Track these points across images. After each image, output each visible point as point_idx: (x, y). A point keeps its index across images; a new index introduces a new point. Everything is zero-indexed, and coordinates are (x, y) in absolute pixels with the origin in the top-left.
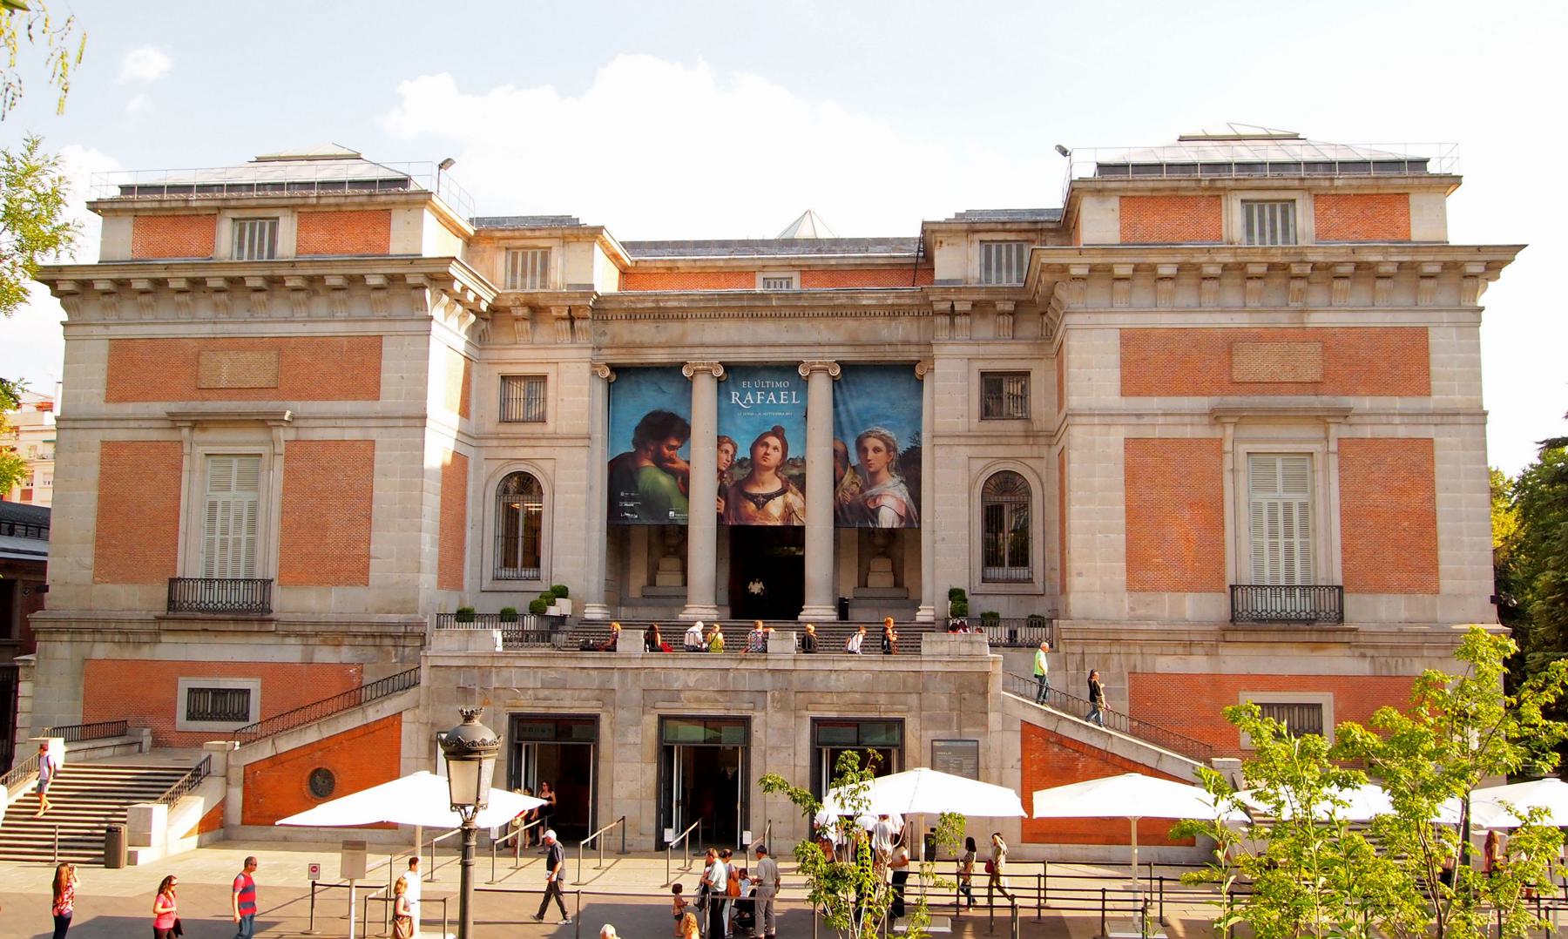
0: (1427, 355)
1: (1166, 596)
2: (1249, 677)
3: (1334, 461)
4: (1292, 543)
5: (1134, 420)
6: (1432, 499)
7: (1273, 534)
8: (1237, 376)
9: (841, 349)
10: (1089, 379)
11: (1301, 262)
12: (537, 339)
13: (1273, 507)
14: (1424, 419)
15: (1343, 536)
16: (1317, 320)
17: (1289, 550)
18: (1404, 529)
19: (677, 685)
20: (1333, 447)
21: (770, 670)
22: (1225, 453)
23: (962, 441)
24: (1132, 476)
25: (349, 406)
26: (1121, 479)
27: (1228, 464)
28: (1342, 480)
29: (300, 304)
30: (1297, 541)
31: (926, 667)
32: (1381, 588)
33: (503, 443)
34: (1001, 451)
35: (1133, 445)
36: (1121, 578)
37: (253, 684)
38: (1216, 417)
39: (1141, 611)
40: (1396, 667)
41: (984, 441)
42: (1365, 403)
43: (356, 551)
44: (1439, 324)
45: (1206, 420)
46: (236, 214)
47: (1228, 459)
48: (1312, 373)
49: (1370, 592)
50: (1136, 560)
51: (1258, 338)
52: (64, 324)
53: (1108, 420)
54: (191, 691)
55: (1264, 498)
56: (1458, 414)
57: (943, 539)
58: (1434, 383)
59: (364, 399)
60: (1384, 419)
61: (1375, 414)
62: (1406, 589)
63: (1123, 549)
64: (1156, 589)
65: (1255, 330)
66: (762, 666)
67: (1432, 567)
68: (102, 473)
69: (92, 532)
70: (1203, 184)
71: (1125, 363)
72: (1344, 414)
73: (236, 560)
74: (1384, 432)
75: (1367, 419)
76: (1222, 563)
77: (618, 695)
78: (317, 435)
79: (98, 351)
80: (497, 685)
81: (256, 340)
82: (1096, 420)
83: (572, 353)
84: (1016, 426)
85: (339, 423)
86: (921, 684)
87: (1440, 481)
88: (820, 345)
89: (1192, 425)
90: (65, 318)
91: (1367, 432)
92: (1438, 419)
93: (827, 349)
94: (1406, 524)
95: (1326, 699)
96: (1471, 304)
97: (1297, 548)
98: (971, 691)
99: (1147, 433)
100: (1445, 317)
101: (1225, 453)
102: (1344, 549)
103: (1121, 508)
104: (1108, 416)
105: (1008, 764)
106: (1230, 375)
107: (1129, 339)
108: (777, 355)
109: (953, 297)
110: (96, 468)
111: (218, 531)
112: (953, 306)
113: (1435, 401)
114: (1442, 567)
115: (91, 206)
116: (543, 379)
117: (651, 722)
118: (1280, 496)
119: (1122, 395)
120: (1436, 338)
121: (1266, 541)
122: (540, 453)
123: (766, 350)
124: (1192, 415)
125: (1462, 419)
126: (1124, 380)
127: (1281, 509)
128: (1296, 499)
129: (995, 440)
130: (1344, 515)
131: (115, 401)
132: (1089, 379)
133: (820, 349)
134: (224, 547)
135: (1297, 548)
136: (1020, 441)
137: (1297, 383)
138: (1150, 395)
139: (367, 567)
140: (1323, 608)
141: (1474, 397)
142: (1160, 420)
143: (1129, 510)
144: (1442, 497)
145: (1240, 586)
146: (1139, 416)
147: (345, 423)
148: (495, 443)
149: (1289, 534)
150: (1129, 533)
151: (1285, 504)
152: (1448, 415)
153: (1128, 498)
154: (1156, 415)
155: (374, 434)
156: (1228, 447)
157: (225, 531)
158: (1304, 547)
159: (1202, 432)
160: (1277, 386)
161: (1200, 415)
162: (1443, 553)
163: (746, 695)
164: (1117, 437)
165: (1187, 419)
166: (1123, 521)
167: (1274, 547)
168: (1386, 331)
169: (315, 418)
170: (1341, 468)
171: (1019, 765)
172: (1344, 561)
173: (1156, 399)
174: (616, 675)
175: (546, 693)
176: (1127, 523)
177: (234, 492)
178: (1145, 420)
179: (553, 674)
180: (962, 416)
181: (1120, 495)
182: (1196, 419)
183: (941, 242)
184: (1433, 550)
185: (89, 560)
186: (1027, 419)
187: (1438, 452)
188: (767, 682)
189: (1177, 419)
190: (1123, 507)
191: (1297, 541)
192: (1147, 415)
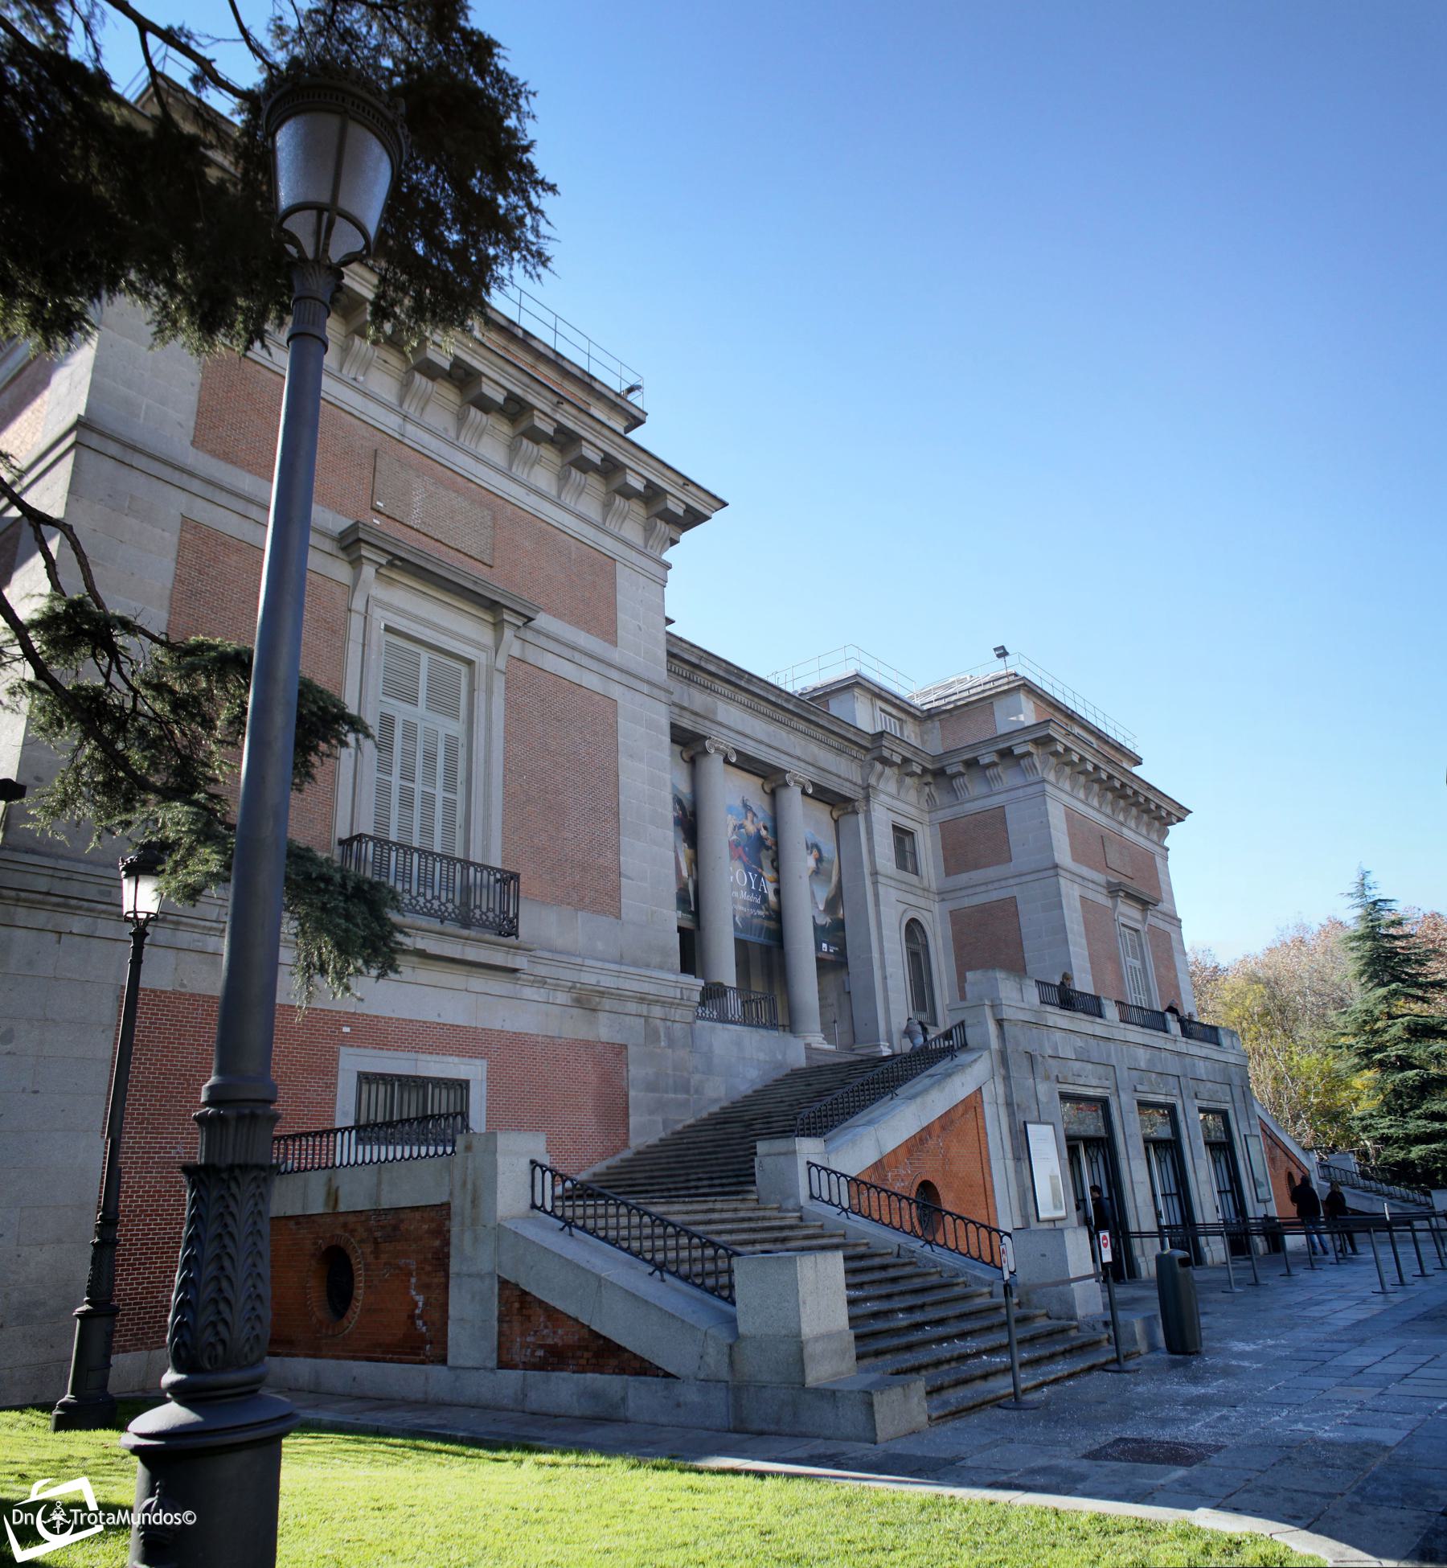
9: (811, 769)
23: (893, 883)
25: (583, 639)
29: (525, 463)
34: (911, 899)
37: (472, 1070)
41: (904, 887)
43: (601, 861)
45: (1105, 891)
54: (365, 1078)
59: (597, 636)
68: (178, 579)
78: (550, 663)
80: (1050, 1052)
81: (459, 479)
84: (912, 878)
85: (577, 657)
111: (396, 770)
129: (908, 888)
131: (213, 453)
134: (407, 801)
136: (920, 892)
139: (618, 888)
147: (585, 661)
155: (616, 692)
157: (408, 775)
169: (548, 636)
186: (916, 872)
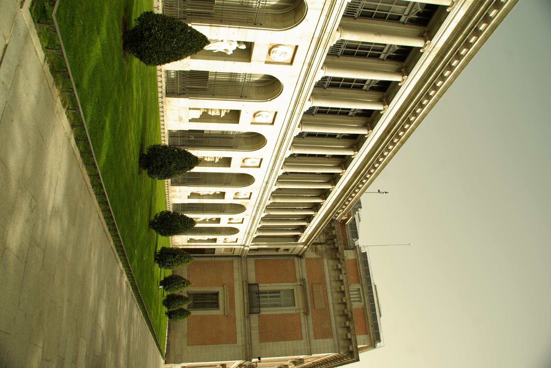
3: (294, 312)
20: (298, 312)
38: (303, 280)
42: (310, 321)
72: (306, 314)
75: (306, 321)
91: (302, 321)
96: (341, 350)
100: (336, 343)
106: (314, 284)
113: (313, 340)
140: (254, 310)
145: (258, 288)
159: (298, 277)
182: (301, 275)
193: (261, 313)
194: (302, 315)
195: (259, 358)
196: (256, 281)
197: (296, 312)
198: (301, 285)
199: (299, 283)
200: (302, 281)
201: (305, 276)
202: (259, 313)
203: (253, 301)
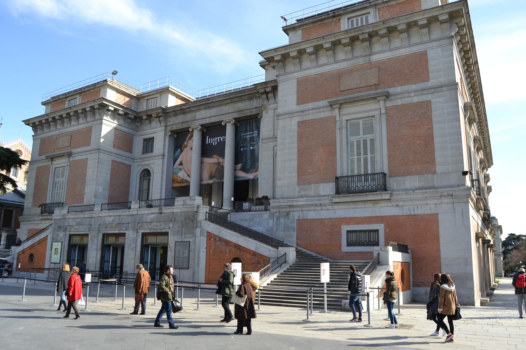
0: (427, 63)
1: (312, 185)
2: (345, 218)
3: (384, 117)
4: (367, 157)
5: (301, 114)
6: (431, 128)
7: (359, 154)
8: (342, 88)
9: (235, 113)
10: (285, 100)
11: (363, 33)
12: (152, 126)
13: (358, 142)
14: (426, 92)
15: (389, 150)
16: (375, 58)
17: (366, 160)
18: (418, 144)
19: (107, 222)
20: (383, 111)
21: (131, 215)
22: (337, 121)
23: (271, 140)
24: (301, 137)
26: (296, 138)
27: (338, 126)
28: (388, 126)
30: (369, 156)
31: (175, 211)
32: (408, 173)
33: (142, 160)
35: (301, 124)
36: (295, 180)
39: (303, 193)
40: (414, 210)
42: (399, 89)
44: (432, 48)
45: (329, 108)
46: (68, 99)
47: (338, 123)
48: (374, 81)
49: (402, 176)
50: (301, 171)
51: (350, 71)
52: (33, 136)
53: (291, 115)
55: (354, 139)
56: (442, 87)
57: (264, 178)
58: (431, 75)
60: (406, 95)
61: (402, 94)
62: (420, 173)
63: (296, 168)
64: (309, 183)
65: (350, 68)
66: (127, 213)
67: (432, 161)
69: (33, 193)
70: (330, 15)
71: (298, 91)
72: (387, 96)
73: (59, 198)
74: (407, 101)
75: (398, 96)
76: (336, 169)
77: (93, 226)
79: (39, 141)
82: (287, 116)
83: (160, 129)
86: (172, 218)
87: (434, 119)
88: (228, 113)
89: (323, 112)
90: (33, 134)
91: (399, 102)
92: (433, 91)
93: (231, 114)
94: (419, 142)
95: (381, 227)
97: (369, 159)
98: (189, 220)
99: (306, 118)
100: (434, 44)
101: (337, 121)
102: (389, 157)
103: (296, 150)
104: (291, 114)
105: (201, 250)
107: (300, 82)
108: (216, 119)
109: (265, 86)
110: (35, 175)
112: (265, 90)
113: (432, 83)
114: (437, 160)
115: (42, 103)
116: (153, 139)
117: (101, 236)
118: (361, 137)
119: (297, 105)
120: (431, 54)
121: (356, 158)
122: (151, 162)
123: (213, 118)
124: (323, 107)
125: (445, 89)
126: (298, 98)
127: (362, 142)
128: (368, 137)
130: (389, 141)
132: (285, 100)
133: (228, 115)
135: (369, 159)
137: (367, 86)
138: (308, 103)
141: (451, 78)
142: (311, 112)
143: (299, 151)
144: (435, 126)
146: (303, 111)
148: (140, 160)
149: (365, 153)
150: (299, 161)
151: (363, 140)
152: (437, 88)
153: (299, 146)
154: (309, 110)
156: (338, 118)
158: (373, 159)
160: (358, 89)
161: (326, 107)
162: (437, 154)
163: (125, 225)
164: (296, 120)
165: (321, 110)
166: (296, 156)
167: (359, 160)
168: (407, 57)
170: (387, 120)
171: (205, 250)
172: (389, 162)
173: (310, 104)
174: (93, 219)
175: (77, 226)
176: (298, 157)
177: (60, 178)
178: (306, 113)
179: (79, 220)
180: (271, 131)
181: (295, 145)
182: (325, 109)
183: (267, 70)
184: (433, 152)
185: (31, 201)
187: (433, 106)
188: (130, 219)
189: (317, 110)
190: (296, 150)
191: (369, 156)
192: (305, 111)
193: (386, 171)
194: (389, 104)
195: (465, 173)
196: (328, 182)
197: (383, 114)
198: (340, 108)
199: (337, 111)
200: (334, 107)
201: (324, 103)
202: (385, 174)
203: (363, 185)
